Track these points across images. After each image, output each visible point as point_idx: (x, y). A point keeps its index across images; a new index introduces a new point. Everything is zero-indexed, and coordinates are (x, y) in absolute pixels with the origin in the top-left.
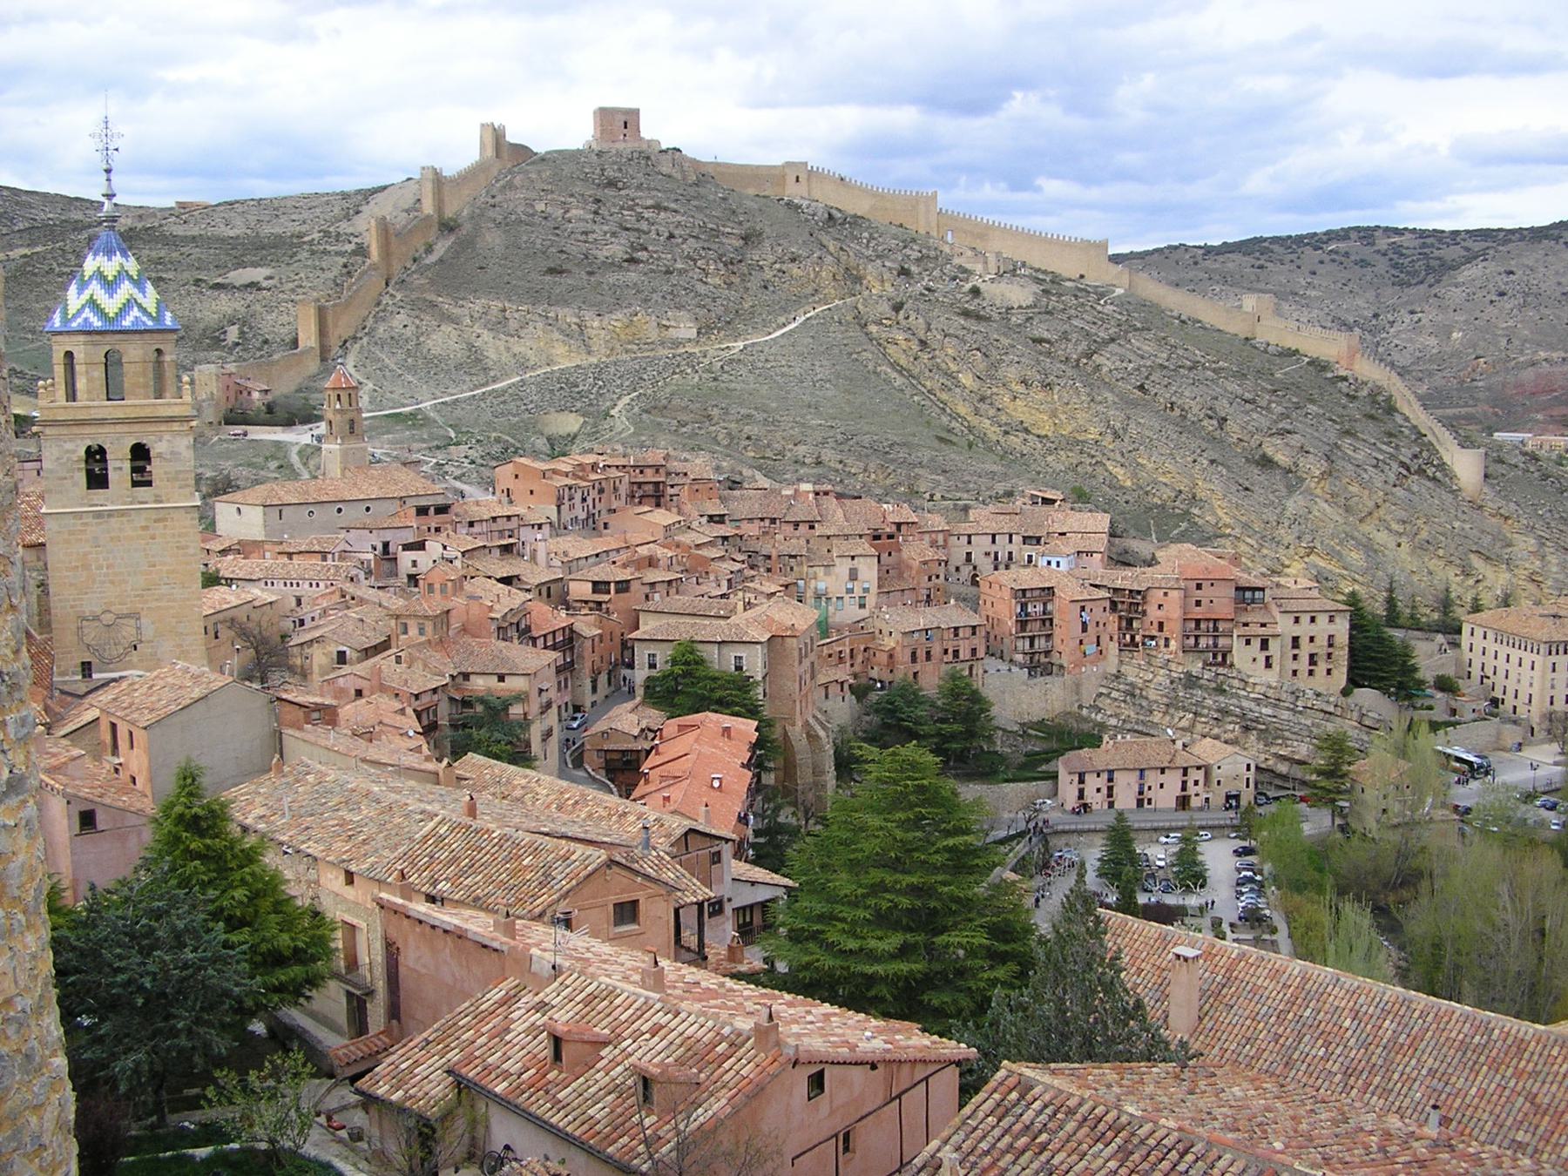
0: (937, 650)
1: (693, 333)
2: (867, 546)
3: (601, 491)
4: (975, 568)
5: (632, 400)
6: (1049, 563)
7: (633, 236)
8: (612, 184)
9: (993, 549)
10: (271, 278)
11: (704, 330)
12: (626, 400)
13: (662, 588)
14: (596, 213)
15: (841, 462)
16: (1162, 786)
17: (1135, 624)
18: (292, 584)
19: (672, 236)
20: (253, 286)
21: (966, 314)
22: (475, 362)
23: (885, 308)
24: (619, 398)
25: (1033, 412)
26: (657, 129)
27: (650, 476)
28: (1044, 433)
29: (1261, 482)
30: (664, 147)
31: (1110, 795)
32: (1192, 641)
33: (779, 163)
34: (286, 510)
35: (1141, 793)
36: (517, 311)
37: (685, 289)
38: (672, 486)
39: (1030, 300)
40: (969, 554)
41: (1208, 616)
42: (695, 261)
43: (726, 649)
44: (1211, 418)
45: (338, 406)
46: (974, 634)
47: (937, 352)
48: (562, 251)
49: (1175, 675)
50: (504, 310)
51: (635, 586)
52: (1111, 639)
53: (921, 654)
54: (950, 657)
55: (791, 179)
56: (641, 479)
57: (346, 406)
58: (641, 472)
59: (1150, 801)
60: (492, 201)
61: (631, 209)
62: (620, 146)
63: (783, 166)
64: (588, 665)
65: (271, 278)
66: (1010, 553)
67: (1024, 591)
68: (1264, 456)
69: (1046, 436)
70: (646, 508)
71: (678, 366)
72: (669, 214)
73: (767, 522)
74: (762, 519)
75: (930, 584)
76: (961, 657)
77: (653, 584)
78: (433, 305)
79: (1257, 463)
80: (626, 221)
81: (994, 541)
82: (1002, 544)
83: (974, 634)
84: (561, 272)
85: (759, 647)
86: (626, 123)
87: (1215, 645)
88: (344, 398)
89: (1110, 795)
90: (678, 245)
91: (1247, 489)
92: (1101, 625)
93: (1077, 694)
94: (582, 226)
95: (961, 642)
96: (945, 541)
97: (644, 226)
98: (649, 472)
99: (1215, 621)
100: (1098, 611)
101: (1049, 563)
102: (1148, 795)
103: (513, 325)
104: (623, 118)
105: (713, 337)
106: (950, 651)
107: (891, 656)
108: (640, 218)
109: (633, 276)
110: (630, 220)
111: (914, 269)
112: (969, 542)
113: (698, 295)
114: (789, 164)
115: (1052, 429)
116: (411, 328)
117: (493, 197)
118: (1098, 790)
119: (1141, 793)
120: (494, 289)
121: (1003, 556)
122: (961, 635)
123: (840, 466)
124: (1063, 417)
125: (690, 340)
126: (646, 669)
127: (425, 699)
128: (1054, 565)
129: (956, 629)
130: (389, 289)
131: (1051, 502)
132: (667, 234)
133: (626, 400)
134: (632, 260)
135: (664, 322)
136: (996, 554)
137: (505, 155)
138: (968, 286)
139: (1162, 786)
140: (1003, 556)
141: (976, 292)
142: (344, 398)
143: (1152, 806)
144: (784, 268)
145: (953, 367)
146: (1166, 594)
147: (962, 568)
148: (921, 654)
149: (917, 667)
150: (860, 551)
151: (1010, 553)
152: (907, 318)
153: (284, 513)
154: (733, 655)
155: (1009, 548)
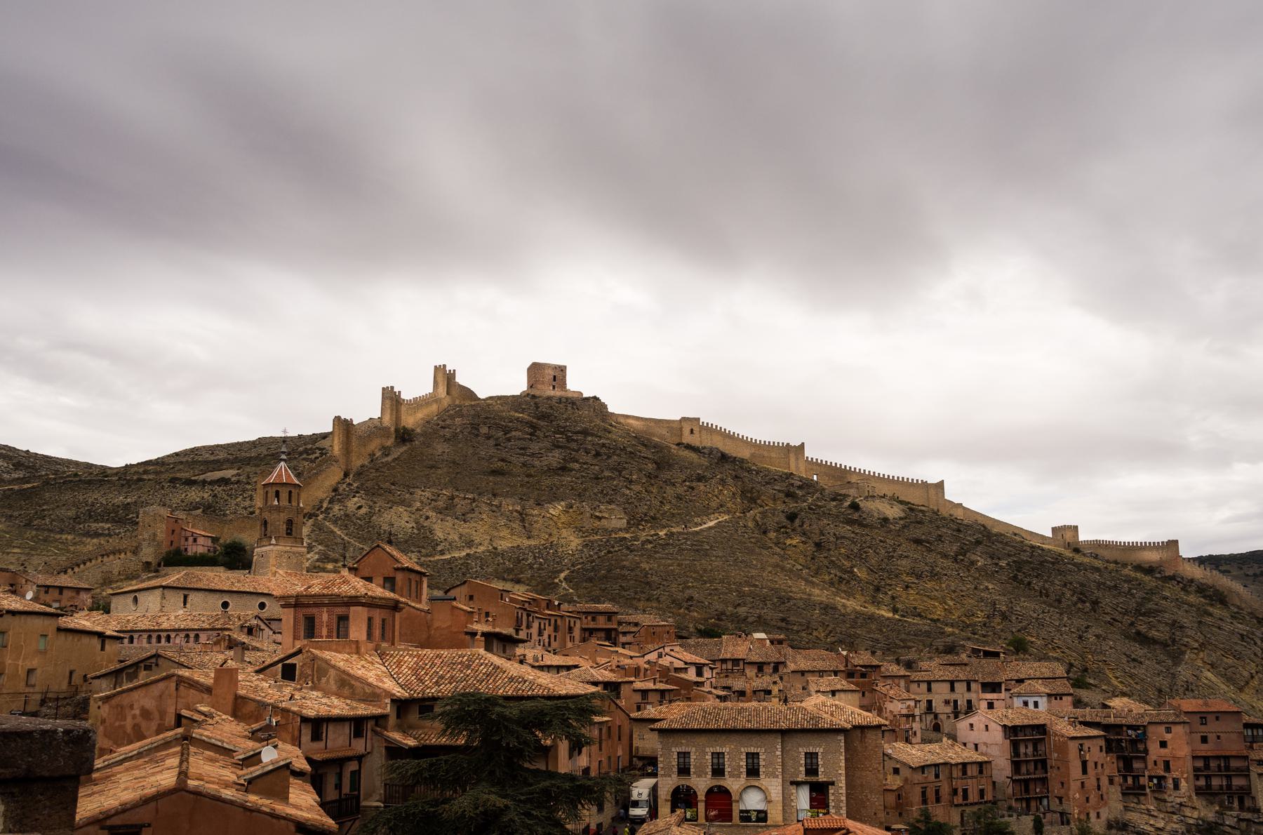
0: (945, 790)
2: (844, 682)
3: (556, 629)
6: (1026, 704)
8: (543, 417)
9: (953, 697)
11: (635, 521)
13: (653, 698)
14: (531, 434)
15: (783, 620)
17: (1137, 765)
18: (159, 638)
20: (224, 481)
21: (851, 522)
23: (783, 518)
25: (925, 599)
26: (577, 384)
27: (602, 622)
28: (936, 617)
30: (585, 396)
32: (1202, 782)
33: (678, 418)
34: (193, 597)
37: (613, 490)
38: (625, 634)
41: (1219, 753)
42: (620, 472)
43: (792, 742)
44: (1084, 602)
46: (981, 772)
47: (832, 553)
49: (1191, 821)
50: (452, 498)
51: (625, 690)
52: (1111, 782)
53: (931, 795)
54: (959, 799)
55: (686, 432)
56: (592, 625)
58: (594, 619)
61: (562, 433)
62: (550, 392)
63: (680, 421)
66: (969, 702)
68: (1138, 633)
69: (938, 620)
70: (607, 643)
71: (613, 547)
73: (730, 666)
74: (724, 661)
76: (971, 799)
77: (645, 693)
79: (1135, 640)
80: (558, 441)
81: (952, 689)
82: (961, 695)
83: (981, 772)
85: (841, 738)
87: (1229, 786)
88: (284, 495)
94: (519, 443)
95: (969, 780)
97: (574, 445)
98: (601, 619)
99: (1227, 758)
100: (1095, 750)
101: (1026, 704)
104: (552, 373)
105: (641, 527)
107: (899, 797)
108: (569, 439)
111: (799, 493)
112: (929, 690)
114: (684, 419)
115: (943, 614)
116: (363, 511)
117: (443, 421)
121: (962, 704)
122: (969, 773)
123: (783, 625)
124: (951, 603)
125: (621, 530)
126: (675, 776)
127: (338, 740)
128: (1031, 706)
129: (964, 765)
130: (347, 480)
131: (996, 655)
132: (594, 452)
134: (563, 469)
135: (597, 514)
136: (956, 702)
137: (455, 392)
140: (962, 704)
141: (855, 507)
142: (284, 495)
144: (694, 484)
145: (847, 564)
148: (931, 795)
150: (839, 687)
151: (969, 702)
152: (801, 526)
153: (189, 599)
154: (802, 750)
155: (968, 696)
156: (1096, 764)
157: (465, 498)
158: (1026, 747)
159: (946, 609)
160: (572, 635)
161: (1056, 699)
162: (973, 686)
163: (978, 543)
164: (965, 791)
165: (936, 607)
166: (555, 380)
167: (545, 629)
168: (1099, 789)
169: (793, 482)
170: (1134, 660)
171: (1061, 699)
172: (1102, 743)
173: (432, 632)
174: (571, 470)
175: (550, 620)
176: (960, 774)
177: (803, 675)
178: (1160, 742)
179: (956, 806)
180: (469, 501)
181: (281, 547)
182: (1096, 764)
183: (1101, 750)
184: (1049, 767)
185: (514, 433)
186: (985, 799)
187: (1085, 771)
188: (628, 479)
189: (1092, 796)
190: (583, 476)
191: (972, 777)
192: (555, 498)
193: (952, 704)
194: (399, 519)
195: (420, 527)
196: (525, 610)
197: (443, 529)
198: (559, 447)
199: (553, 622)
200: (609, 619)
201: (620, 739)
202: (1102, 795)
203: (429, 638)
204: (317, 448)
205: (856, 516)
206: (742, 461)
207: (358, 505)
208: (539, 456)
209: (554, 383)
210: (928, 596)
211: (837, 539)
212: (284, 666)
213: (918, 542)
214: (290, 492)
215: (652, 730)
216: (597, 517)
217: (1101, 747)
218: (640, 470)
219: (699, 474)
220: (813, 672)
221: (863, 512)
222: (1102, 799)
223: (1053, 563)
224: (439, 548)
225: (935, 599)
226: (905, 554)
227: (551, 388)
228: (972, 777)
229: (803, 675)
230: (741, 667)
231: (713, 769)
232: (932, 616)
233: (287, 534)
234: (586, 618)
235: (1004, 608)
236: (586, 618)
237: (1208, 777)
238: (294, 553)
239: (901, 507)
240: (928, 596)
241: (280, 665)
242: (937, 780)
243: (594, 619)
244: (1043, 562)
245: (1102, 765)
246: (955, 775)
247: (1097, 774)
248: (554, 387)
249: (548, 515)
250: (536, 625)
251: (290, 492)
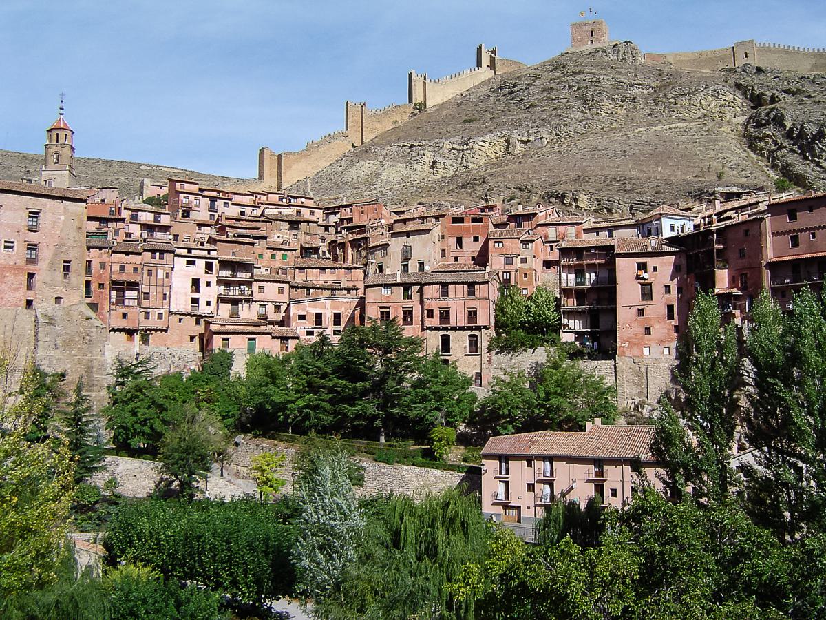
46: (472, 293)
57: (55, 143)
83: (472, 293)
93: (638, 384)
106: (436, 312)
122: (451, 294)
166: (592, 35)
176: (438, 295)
177: (405, 223)
186: (478, 324)
189: (657, 326)
191: (455, 299)
209: (592, 38)
214: (66, 135)
220: (414, 219)
227: (589, 43)
228: (455, 299)
229: (405, 223)
238: (58, 175)
248: (592, 41)
249: (478, 147)
251: (57, 134)
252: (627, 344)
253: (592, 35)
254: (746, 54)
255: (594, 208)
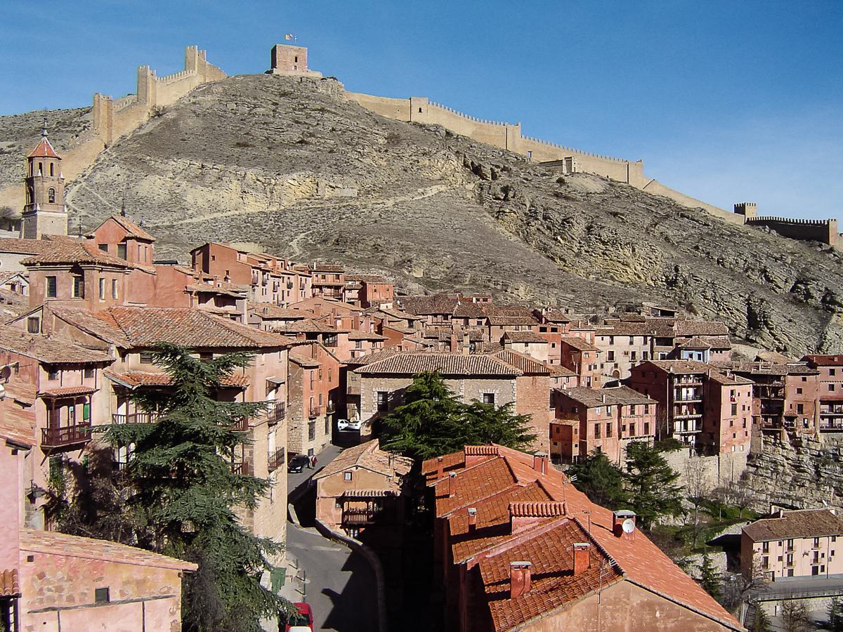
1: (354, 193)
4: (616, 366)
5: (307, 235)
7: (303, 128)
9: (632, 349)
10: (13, 146)
12: (302, 235)
16: (833, 553)
19: (333, 130)
21: (557, 195)
22: (175, 202)
24: (296, 235)
25: (620, 265)
27: (330, 280)
29: (799, 316)
31: (790, 564)
35: (816, 560)
36: (213, 170)
39: (601, 189)
40: (611, 354)
45: (40, 174)
48: (247, 134)
53: (603, 429)
54: (626, 434)
55: (415, 110)
56: (322, 282)
58: (324, 277)
59: (823, 570)
60: (193, 100)
62: (292, 73)
64: (306, 402)
65: (13, 146)
66: (645, 354)
67: (679, 377)
71: (344, 214)
72: (330, 115)
75: (590, 374)
78: (143, 162)
83: (647, 412)
84: (248, 146)
86: (296, 58)
88: (47, 168)
89: (790, 564)
90: (338, 135)
91: (790, 321)
92: (746, 409)
96: (592, 340)
101: (691, 356)
102: (823, 561)
103: (208, 180)
106: (628, 427)
108: (309, 116)
109: (304, 152)
110: (301, 116)
111: (514, 169)
112: (612, 343)
113: (355, 168)
118: (780, 559)
119: (816, 560)
120: (192, 153)
122: (636, 413)
124: (639, 268)
127: (71, 381)
128: (695, 358)
133: (302, 235)
136: (633, 353)
138: (555, 179)
139: (833, 553)
141: (561, 181)
142: (47, 168)
143: (825, 573)
146: (804, 379)
147: (605, 365)
148: (603, 429)
149: (600, 442)
156: (744, 406)
157: (213, 168)
158: (688, 392)
159: (635, 274)
160: (304, 291)
161: (717, 352)
162: (649, 338)
163: (667, 216)
164: (632, 427)
165: (627, 272)
166: (296, 61)
167: (279, 286)
168: (744, 427)
169: (509, 158)
170: (790, 321)
171: (721, 352)
172: (750, 388)
173: (158, 291)
174: (307, 143)
175: (283, 278)
176: (629, 413)
177: (501, 328)
178: (801, 389)
179: (624, 439)
180: (216, 171)
181: (45, 213)
182: (744, 406)
183: (749, 395)
184: (705, 409)
185: (258, 110)
187: (734, 412)
188: (360, 152)
189: (738, 432)
190: (319, 150)
192: (292, 168)
193: (630, 355)
194: (153, 186)
195: (171, 192)
196: (260, 269)
197: (195, 196)
198: (297, 122)
199: (286, 279)
200: (338, 277)
201: (330, 381)
202: (746, 432)
203: (155, 295)
204: (81, 122)
205: (562, 190)
206: (465, 139)
207: (117, 174)
208: (281, 130)
210: (619, 262)
211: (544, 210)
212: (29, 318)
213: (615, 214)
214: (52, 164)
215: (356, 373)
216: (331, 187)
217: (749, 393)
218: (373, 144)
219: (424, 150)
221: (568, 187)
222: (746, 435)
223: (729, 236)
224: (190, 212)
225: (628, 265)
226: (603, 224)
227: (293, 68)
230: (450, 320)
231: (378, 405)
232: (622, 280)
233: (50, 202)
234: (317, 276)
235: (686, 274)
236: (317, 276)
237: (831, 418)
238: (57, 218)
239: (603, 182)
240: (619, 262)
241: (26, 318)
242: (609, 417)
243: (324, 277)
244: (722, 234)
245: (749, 407)
246: (623, 414)
247: (744, 415)
250: (271, 281)
251: (52, 164)
252: (724, 445)
253: (296, 61)
254: (420, 109)
255: (528, 298)
